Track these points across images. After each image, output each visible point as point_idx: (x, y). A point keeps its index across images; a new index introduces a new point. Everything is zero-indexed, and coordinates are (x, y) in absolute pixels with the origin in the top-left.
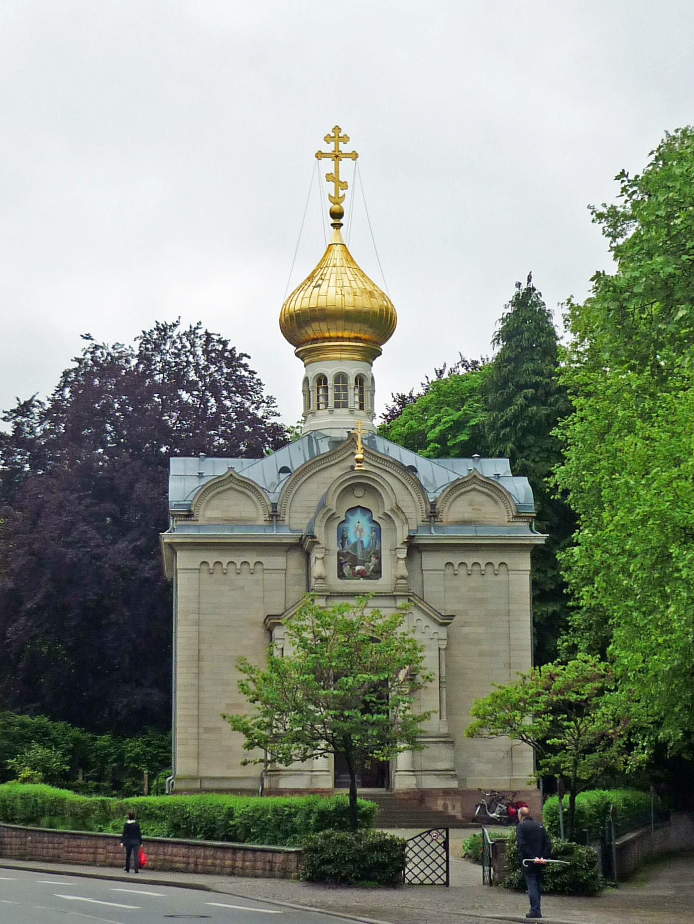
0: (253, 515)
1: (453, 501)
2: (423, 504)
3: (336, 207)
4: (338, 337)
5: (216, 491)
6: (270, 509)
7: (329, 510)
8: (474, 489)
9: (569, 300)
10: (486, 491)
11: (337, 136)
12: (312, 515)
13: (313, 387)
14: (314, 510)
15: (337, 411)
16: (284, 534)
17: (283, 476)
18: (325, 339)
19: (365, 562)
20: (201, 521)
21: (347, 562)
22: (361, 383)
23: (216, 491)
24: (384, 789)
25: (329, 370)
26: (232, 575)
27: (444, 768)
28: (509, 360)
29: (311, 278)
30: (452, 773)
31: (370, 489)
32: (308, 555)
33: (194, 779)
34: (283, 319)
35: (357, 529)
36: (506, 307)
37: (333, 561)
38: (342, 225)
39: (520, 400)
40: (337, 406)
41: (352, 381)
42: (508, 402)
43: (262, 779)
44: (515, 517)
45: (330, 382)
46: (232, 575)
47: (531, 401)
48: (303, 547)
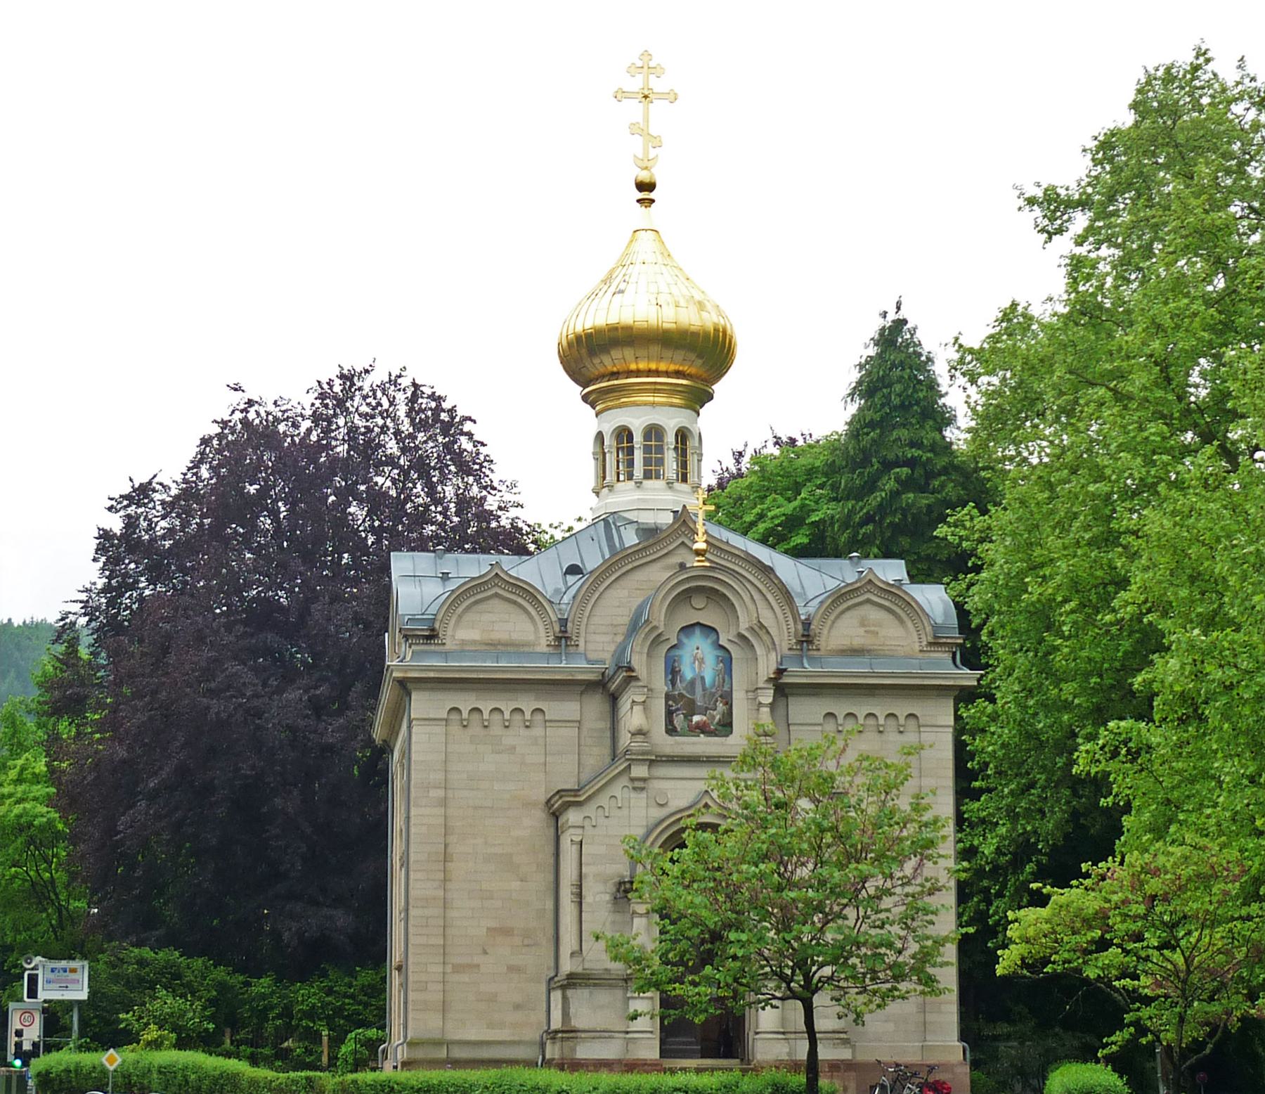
0: (532, 638)
1: (833, 622)
2: (791, 622)
3: (644, 176)
4: (650, 371)
5: (472, 599)
6: (557, 628)
7: (655, 628)
8: (868, 601)
9: (957, 339)
10: (887, 603)
11: (646, 66)
12: (620, 639)
13: (610, 446)
14: (623, 630)
15: (647, 483)
16: (577, 666)
17: (571, 579)
18: (630, 374)
19: (707, 709)
20: (450, 645)
21: (680, 708)
22: (684, 442)
23: (472, 599)
24: (738, 1061)
25: (637, 421)
26: (496, 730)
27: (830, 1028)
28: (872, 425)
29: (607, 280)
30: (842, 1036)
31: (715, 596)
32: (614, 699)
33: (437, 1043)
34: (564, 343)
35: (695, 658)
36: (867, 347)
37: (659, 707)
38: (653, 201)
39: (889, 484)
40: (648, 475)
41: (670, 439)
42: (871, 486)
43: (543, 1046)
44: (930, 644)
45: (638, 439)
46: (496, 730)
47: (906, 485)
48: (607, 688)
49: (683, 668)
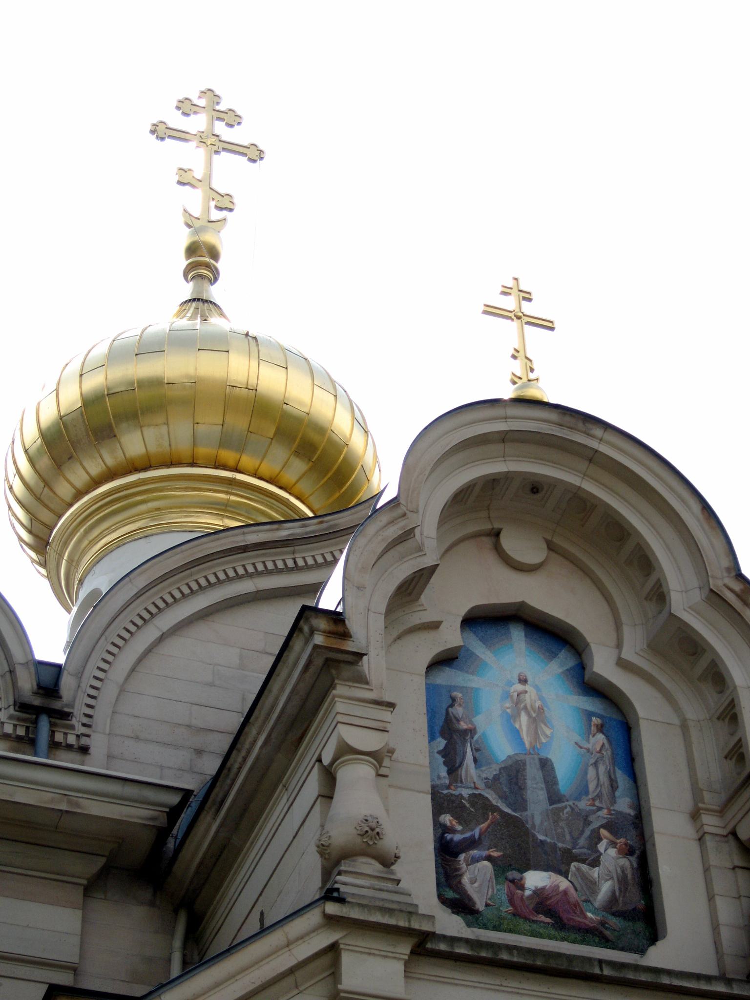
19: (569, 857)
49: (479, 721)
